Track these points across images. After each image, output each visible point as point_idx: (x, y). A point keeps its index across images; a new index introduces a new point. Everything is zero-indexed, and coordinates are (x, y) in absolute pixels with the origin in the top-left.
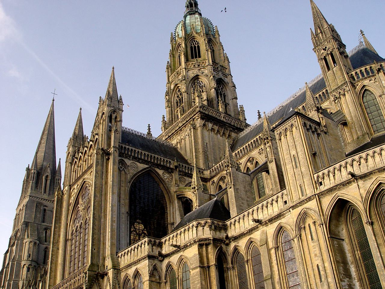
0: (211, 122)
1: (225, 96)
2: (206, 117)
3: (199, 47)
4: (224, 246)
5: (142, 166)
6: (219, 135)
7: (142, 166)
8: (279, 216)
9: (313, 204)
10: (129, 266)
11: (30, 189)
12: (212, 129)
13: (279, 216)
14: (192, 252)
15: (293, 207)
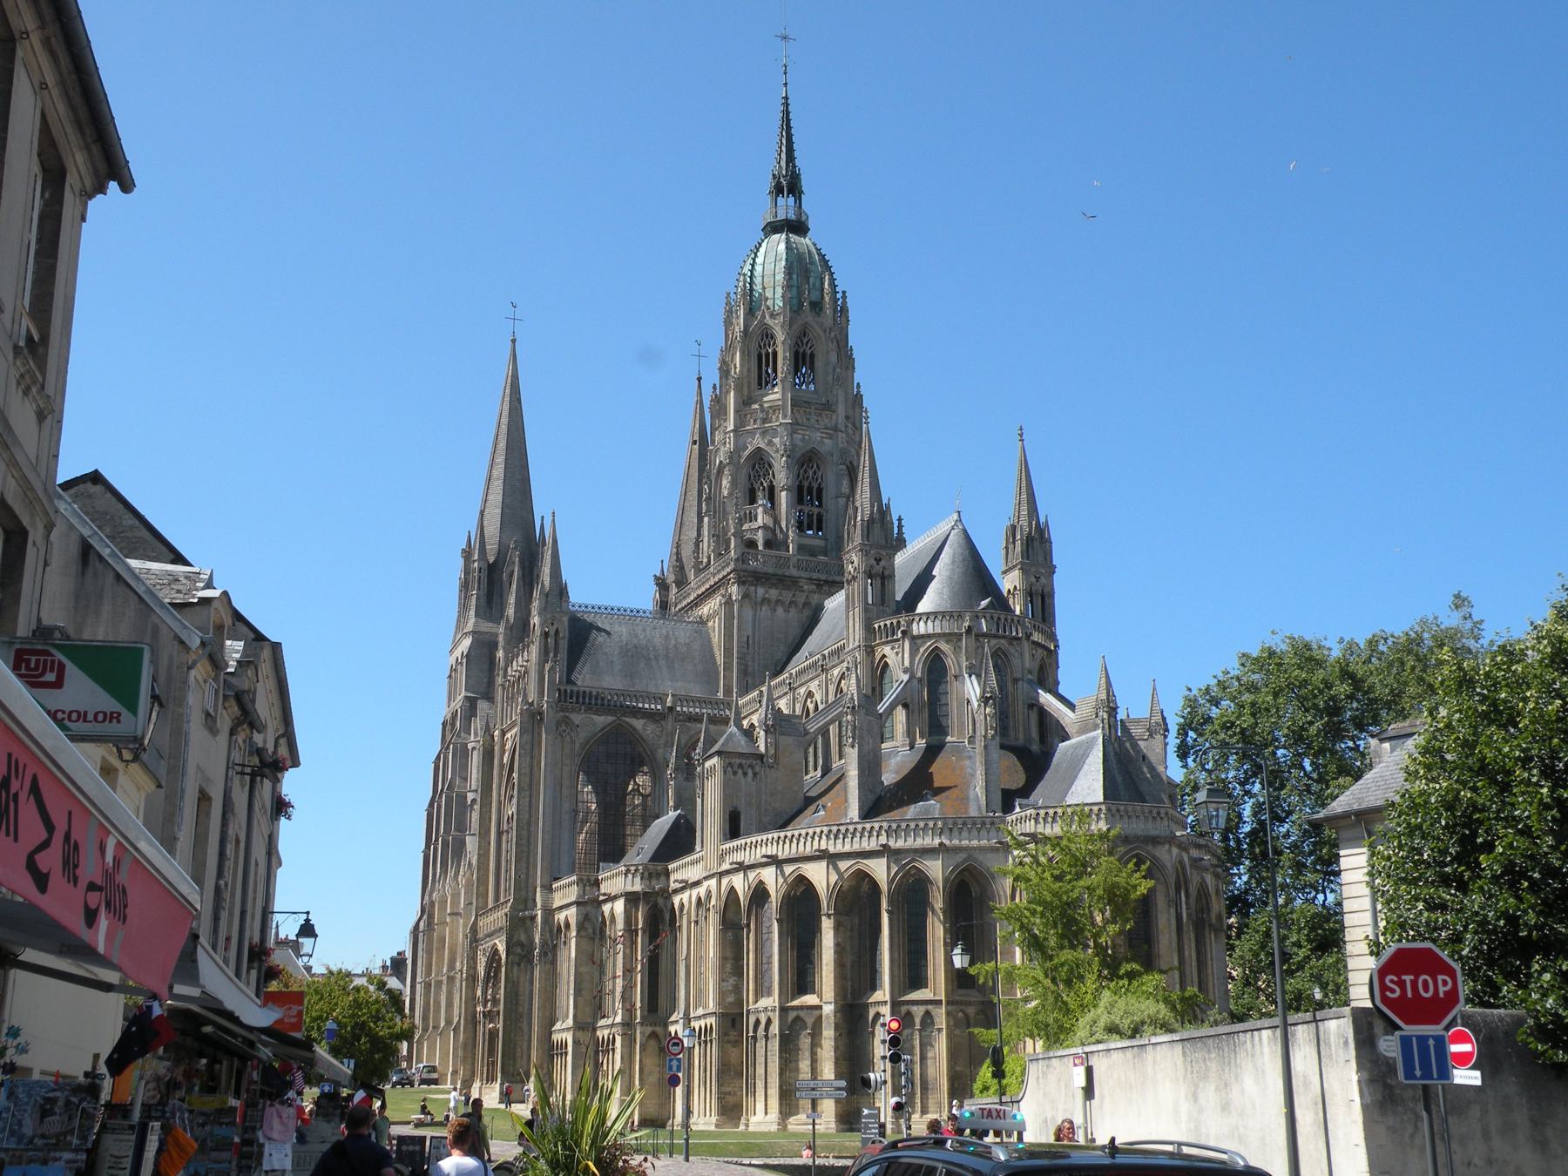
0: (763, 584)
1: (820, 491)
2: (748, 578)
3: (775, 353)
4: (660, 901)
5: (601, 720)
6: (780, 610)
7: (601, 720)
8: (697, 883)
9: (713, 882)
10: (561, 908)
11: (472, 613)
12: (764, 600)
13: (697, 883)
14: (619, 906)
15: (706, 878)
